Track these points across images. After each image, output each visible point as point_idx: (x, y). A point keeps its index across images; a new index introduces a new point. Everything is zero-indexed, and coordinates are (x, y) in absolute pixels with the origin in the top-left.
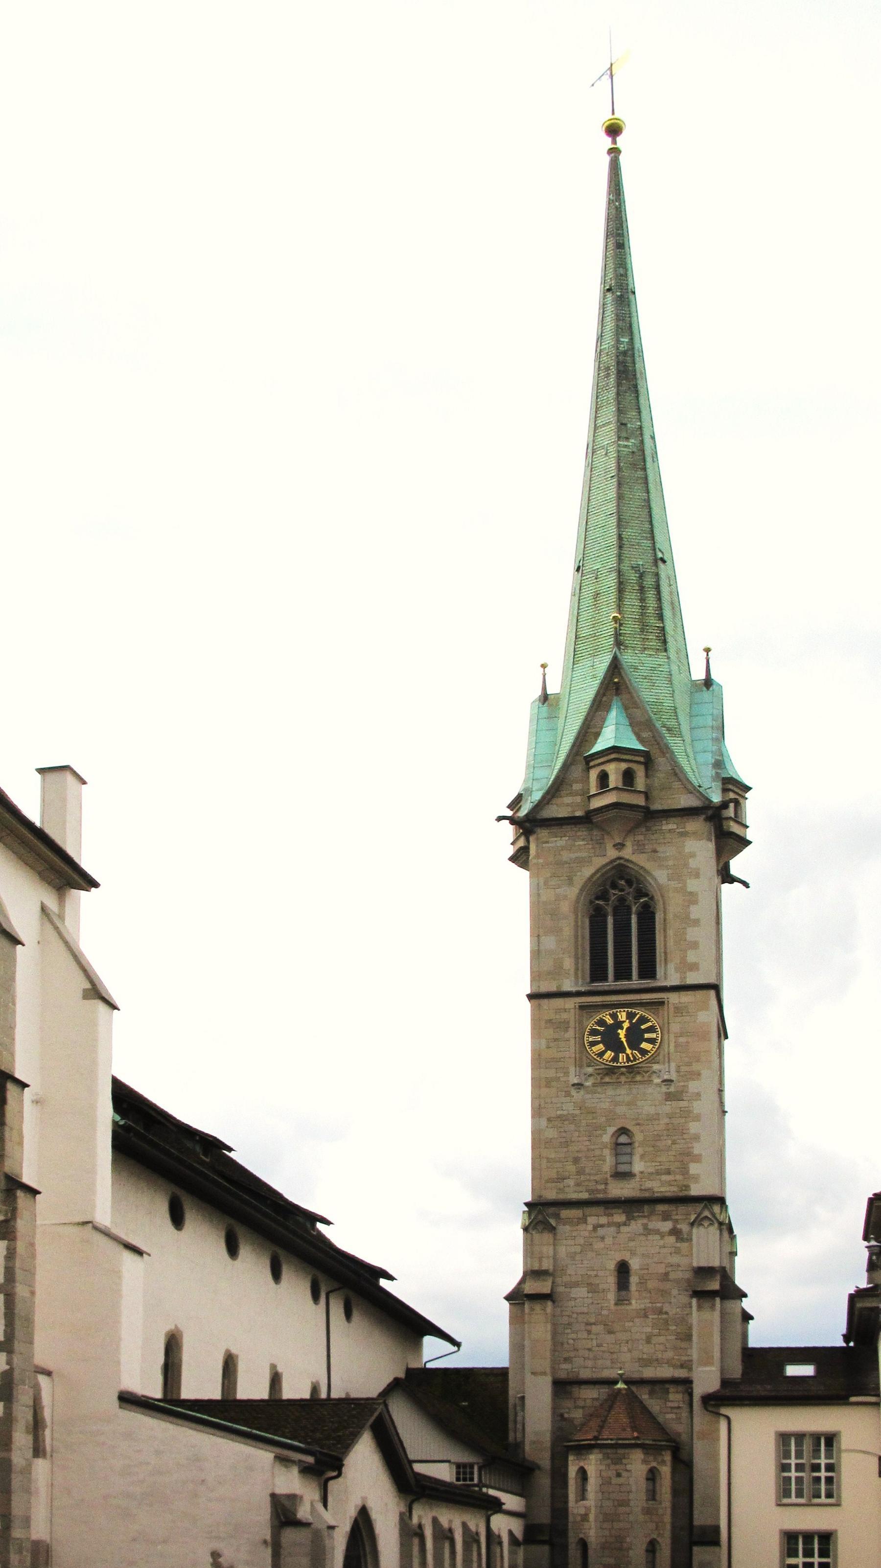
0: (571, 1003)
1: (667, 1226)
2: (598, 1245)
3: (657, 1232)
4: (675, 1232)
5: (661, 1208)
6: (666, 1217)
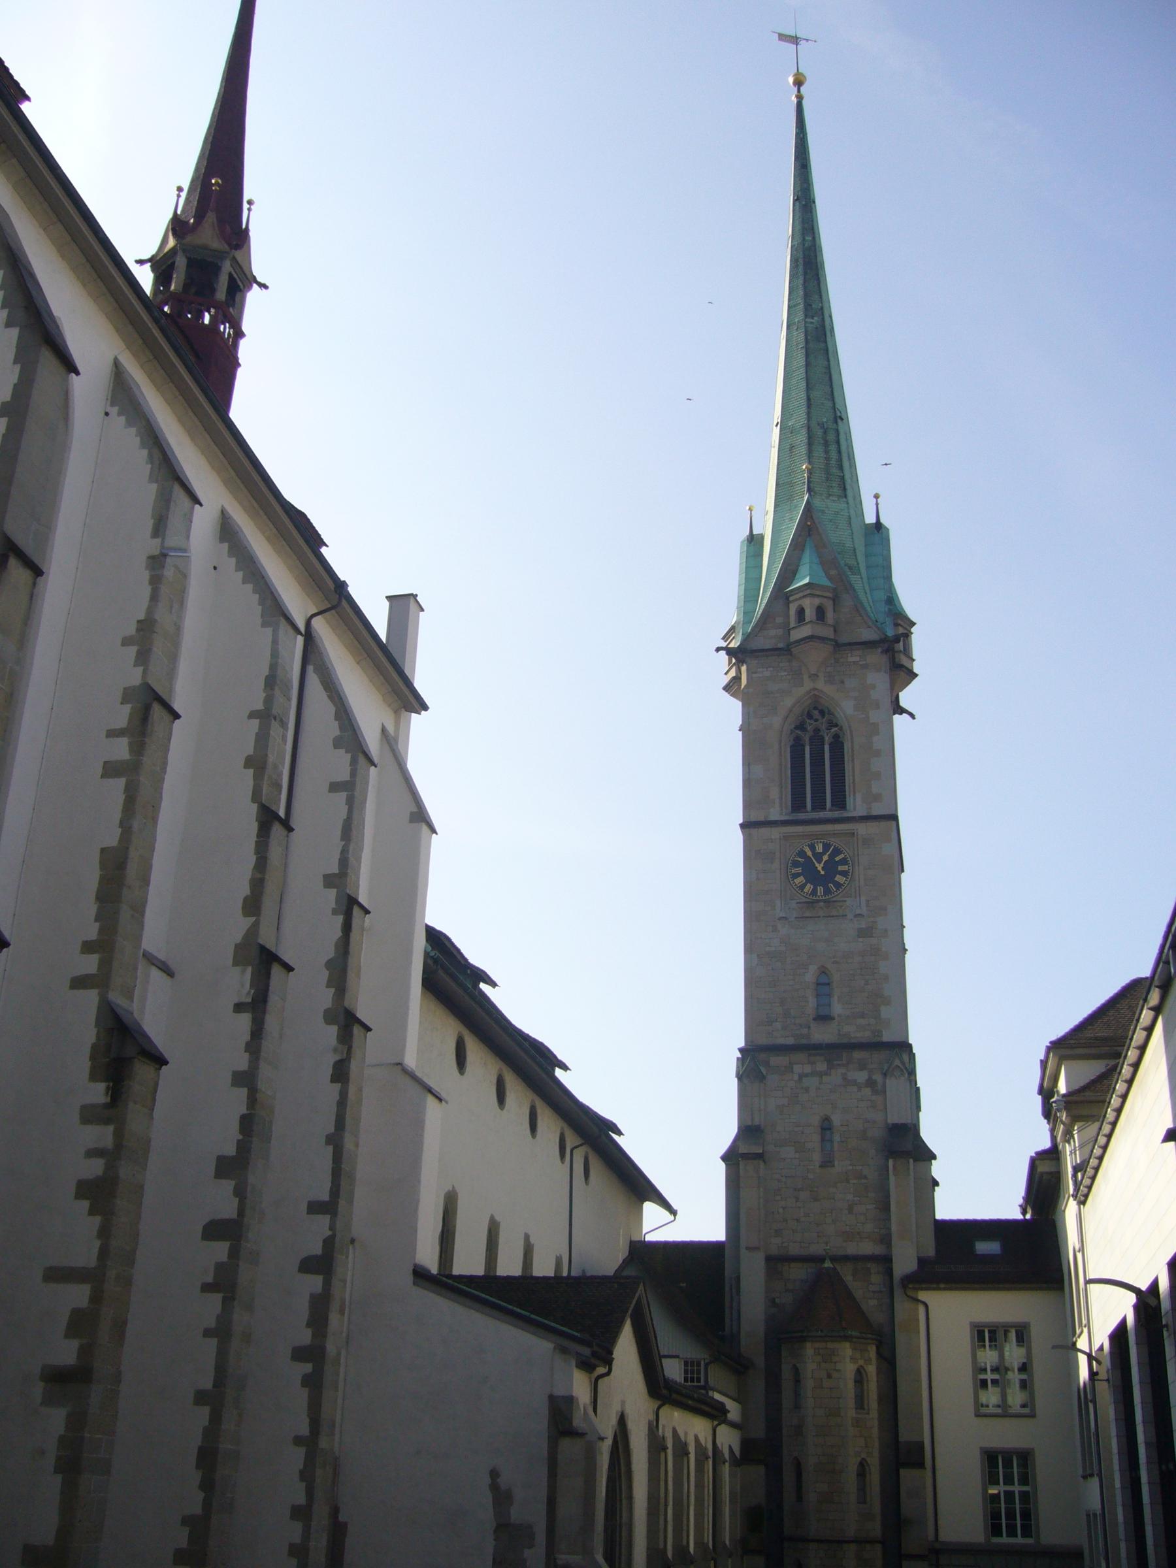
0: (775, 833)
4: (871, 1083)
5: (858, 1055)
6: (862, 1067)
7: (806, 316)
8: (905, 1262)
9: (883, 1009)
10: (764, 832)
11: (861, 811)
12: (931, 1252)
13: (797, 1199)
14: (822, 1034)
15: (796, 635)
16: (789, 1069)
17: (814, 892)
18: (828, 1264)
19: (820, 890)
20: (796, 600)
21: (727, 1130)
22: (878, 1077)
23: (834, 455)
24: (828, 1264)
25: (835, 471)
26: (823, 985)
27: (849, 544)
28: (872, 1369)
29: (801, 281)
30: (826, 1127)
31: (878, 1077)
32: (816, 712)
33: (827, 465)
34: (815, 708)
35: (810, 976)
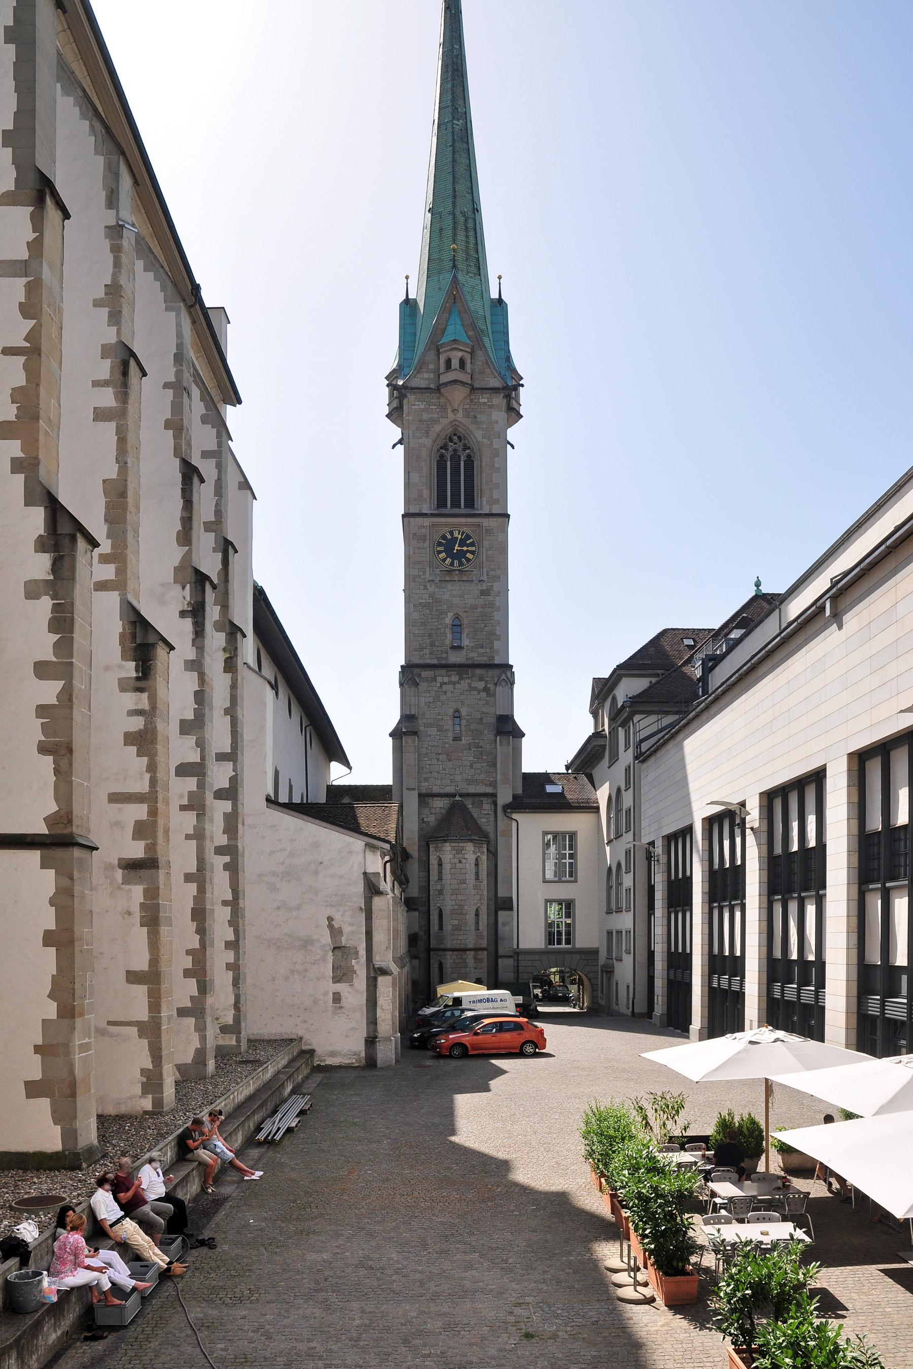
0: (427, 522)
1: (481, 685)
2: (443, 697)
3: (476, 689)
4: (486, 689)
5: (478, 671)
6: (481, 679)
7: (454, 118)
8: (505, 797)
9: (495, 642)
10: (419, 520)
12: (520, 791)
13: (438, 759)
14: (455, 658)
15: (445, 378)
16: (434, 679)
17: (452, 564)
18: (457, 798)
19: (456, 562)
20: (446, 351)
21: (393, 717)
23: (472, 239)
24: (457, 798)
25: (472, 252)
26: (457, 626)
27: (481, 312)
28: (484, 857)
29: (449, 86)
31: (491, 686)
32: (456, 438)
34: (455, 435)
35: (448, 620)
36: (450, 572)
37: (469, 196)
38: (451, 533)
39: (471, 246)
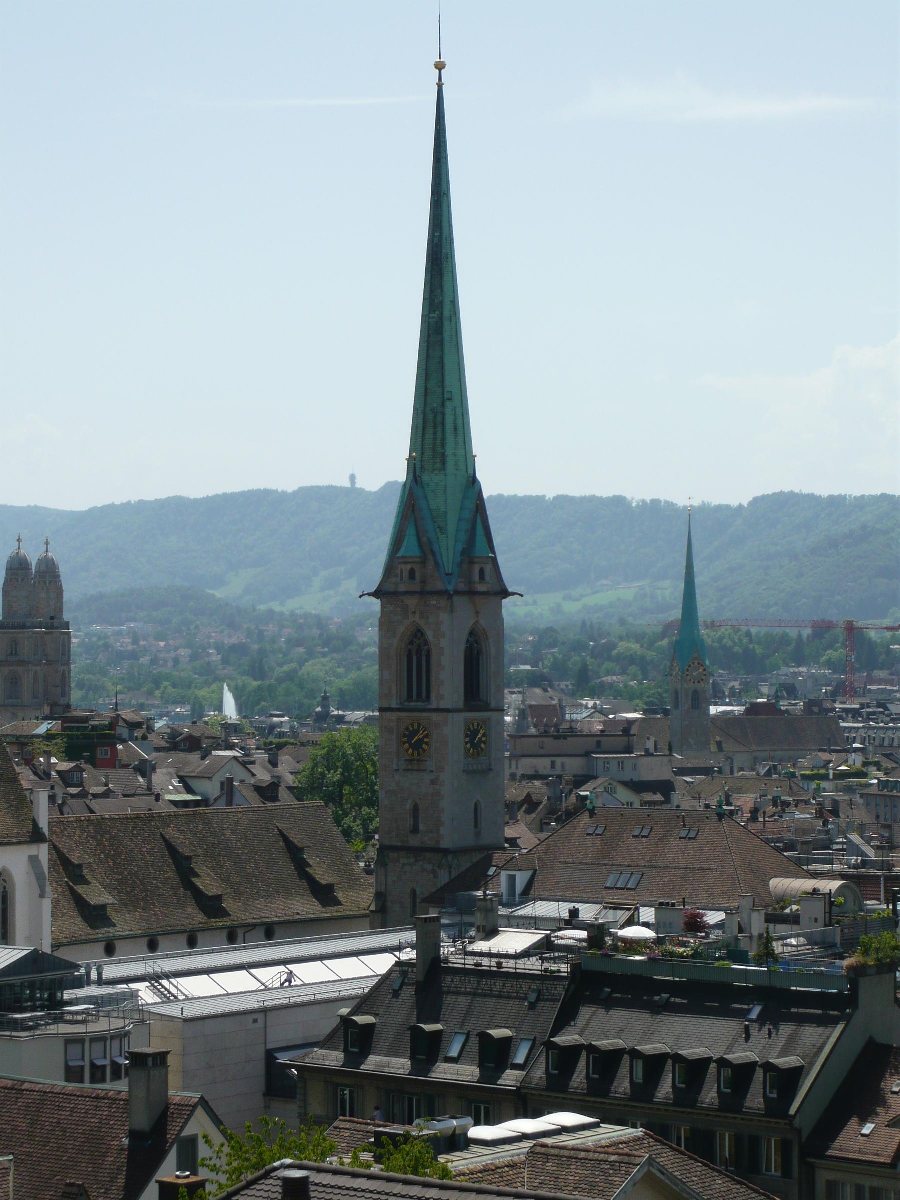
0: (394, 716)
1: (429, 867)
4: (434, 872)
5: (428, 855)
7: (430, 313)
11: (434, 706)
14: (414, 842)
17: (413, 755)
19: (416, 752)
22: (436, 868)
23: (439, 435)
30: (414, 893)
31: (436, 868)
33: (434, 444)
35: (409, 806)
36: (411, 761)
37: (439, 390)
38: (413, 726)
39: (439, 442)
